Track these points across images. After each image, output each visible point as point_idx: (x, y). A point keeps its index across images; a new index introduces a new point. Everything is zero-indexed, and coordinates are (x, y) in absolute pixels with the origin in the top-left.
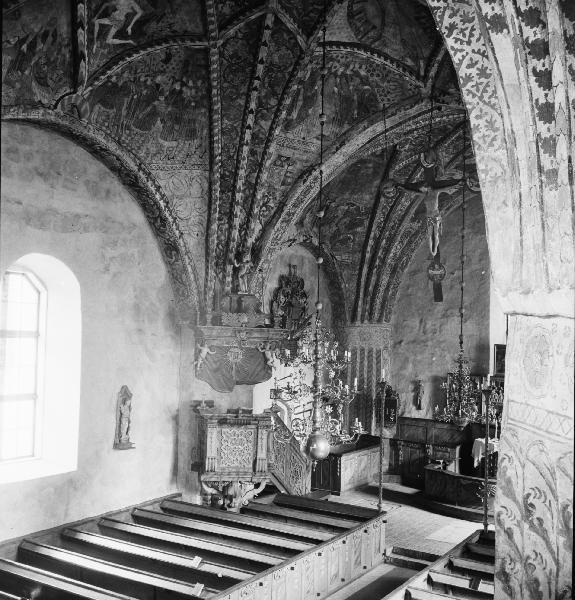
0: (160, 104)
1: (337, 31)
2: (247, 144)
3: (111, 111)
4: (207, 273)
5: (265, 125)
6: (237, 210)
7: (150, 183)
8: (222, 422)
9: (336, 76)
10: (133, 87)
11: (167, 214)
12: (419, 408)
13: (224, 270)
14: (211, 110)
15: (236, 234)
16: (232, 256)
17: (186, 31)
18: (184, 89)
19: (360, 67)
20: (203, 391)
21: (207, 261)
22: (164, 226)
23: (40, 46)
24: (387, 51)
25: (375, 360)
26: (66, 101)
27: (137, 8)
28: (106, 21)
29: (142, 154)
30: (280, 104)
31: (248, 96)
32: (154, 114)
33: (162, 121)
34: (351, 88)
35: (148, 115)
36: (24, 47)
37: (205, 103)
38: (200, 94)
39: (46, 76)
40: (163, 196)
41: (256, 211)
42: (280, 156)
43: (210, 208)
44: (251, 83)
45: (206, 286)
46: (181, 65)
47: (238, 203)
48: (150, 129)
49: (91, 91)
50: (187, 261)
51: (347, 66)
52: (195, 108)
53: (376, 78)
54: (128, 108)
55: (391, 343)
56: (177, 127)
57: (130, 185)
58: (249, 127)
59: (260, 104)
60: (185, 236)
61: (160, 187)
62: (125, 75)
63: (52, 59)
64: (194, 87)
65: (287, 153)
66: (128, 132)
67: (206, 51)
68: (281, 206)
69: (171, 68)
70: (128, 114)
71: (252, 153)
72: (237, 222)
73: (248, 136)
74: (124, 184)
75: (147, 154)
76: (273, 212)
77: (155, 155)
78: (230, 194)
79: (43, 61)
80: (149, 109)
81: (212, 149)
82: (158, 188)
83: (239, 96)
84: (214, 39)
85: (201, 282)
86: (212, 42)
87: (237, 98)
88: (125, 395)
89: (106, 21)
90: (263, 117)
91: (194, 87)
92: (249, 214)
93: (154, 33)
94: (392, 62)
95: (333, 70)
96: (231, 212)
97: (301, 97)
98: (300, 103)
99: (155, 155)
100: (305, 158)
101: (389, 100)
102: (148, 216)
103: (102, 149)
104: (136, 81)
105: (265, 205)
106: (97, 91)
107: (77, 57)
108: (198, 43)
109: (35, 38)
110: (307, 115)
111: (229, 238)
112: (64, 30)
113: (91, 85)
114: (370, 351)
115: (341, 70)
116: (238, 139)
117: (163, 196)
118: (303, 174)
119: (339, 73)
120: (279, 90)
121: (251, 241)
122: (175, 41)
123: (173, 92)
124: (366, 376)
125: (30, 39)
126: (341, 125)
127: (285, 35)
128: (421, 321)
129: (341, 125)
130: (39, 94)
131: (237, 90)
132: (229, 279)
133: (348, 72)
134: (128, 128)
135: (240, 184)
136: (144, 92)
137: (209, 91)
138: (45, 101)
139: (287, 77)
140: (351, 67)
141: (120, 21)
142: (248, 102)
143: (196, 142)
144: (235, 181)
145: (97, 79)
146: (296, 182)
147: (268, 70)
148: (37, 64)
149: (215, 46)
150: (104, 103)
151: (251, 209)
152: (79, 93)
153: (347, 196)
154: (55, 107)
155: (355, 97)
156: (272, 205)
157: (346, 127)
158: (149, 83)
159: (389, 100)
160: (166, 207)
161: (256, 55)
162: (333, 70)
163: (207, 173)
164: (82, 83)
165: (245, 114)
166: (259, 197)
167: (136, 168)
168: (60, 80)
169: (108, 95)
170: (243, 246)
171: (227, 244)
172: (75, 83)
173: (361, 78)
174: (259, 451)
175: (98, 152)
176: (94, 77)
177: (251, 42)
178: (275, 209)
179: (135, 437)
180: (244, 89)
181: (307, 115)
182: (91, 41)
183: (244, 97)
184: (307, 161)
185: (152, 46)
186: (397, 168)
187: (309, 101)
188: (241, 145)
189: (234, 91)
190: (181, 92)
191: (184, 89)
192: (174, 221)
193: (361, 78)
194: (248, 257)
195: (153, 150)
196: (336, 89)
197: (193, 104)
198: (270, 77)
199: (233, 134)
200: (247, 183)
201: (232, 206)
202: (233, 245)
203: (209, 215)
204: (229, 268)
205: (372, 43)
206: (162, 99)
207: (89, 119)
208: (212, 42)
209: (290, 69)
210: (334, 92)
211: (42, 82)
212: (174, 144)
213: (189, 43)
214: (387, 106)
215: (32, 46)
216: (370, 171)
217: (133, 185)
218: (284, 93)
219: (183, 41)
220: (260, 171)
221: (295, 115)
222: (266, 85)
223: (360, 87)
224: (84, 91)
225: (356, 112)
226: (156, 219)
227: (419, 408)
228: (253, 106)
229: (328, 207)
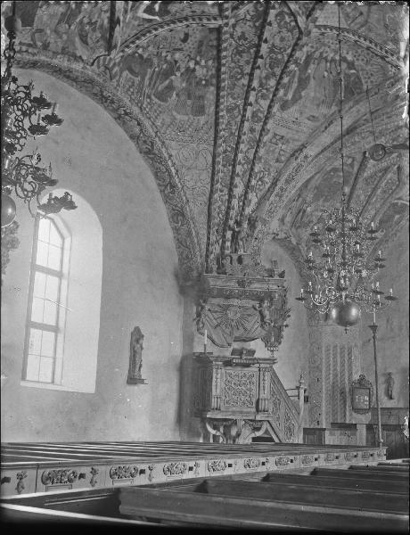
0: (177, 80)
1: (331, 16)
2: (248, 120)
3: (136, 79)
4: (209, 239)
5: (265, 104)
6: (237, 180)
7: (164, 150)
8: (228, 363)
9: (326, 59)
10: (155, 61)
11: (177, 180)
12: (391, 398)
13: (224, 236)
14: (218, 88)
15: (235, 202)
16: (231, 222)
17: (204, 12)
18: (197, 67)
20: (201, 345)
21: (209, 227)
22: (173, 192)
24: (372, 35)
25: (346, 355)
26: (101, 62)
29: (158, 123)
30: (278, 83)
31: (251, 75)
32: (170, 88)
33: (177, 95)
35: (167, 87)
37: (214, 81)
38: (210, 73)
40: (174, 164)
41: (253, 182)
42: (275, 135)
43: (212, 179)
44: (255, 63)
45: (207, 250)
46: (196, 45)
47: (238, 175)
48: (165, 101)
49: (122, 57)
50: (192, 226)
52: (205, 85)
54: (151, 79)
55: (360, 343)
56: (189, 102)
57: (146, 153)
58: (251, 104)
59: (261, 85)
60: (191, 204)
61: (171, 156)
62: (150, 48)
63: (93, 21)
64: (205, 67)
65: (282, 132)
66: (148, 100)
67: (219, 30)
68: (274, 184)
69: (187, 48)
70: (150, 83)
71: (252, 130)
72: (239, 191)
73: (249, 114)
74: (141, 152)
75: (163, 124)
76: (267, 186)
77: (169, 126)
78: (230, 168)
79: (86, 20)
80: (167, 82)
81: (217, 124)
82: (170, 156)
83: (243, 75)
84: (227, 17)
85: (204, 247)
86: (225, 21)
87: (241, 78)
88: (137, 336)
90: (264, 97)
91: (205, 67)
92: (247, 186)
93: (176, 11)
94: (376, 45)
95: (325, 55)
96: (231, 184)
97: (296, 80)
99: (169, 126)
100: (297, 137)
101: (372, 82)
102: (159, 185)
103: (126, 114)
104: (158, 55)
105: (260, 179)
106: (126, 58)
107: (114, 22)
108: (213, 21)
110: (301, 97)
111: (229, 208)
113: (123, 51)
114: (342, 348)
115: (332, 55)
116: (240, 117)
117: (174, 164)
118: (293, 155)
119: (329, 58)
120: (278, 71)
121: (248, 211)
122: (194, 20)
123: (188, 69)
124: (338, 369)
127: (287, 17)
128: (388, 321)
130: (81, 51)
131: (241, 70)
132: (228, 244)
133: (337, 58)
134: (149, 97)
135: (240, 156)
136: (164, 67)
137: (218, 70)
138: (85, 58)
139: (286, 58)
142: (251, 81)
143: (202, 119)
144: (236, 155)
145: (128, 47)
146: (288, 160)
147: (271, 50)
148: (81, 22)
149: (227, 24)
150: (132, 71)
151: (249, 181)
152: (112, 56)
153: (321, 203)
154: (93, 64)
156: (266, 180)
158: (169, 58)
159: (372, 82)
160: (176, 174)
161: (260, 38)
162: (325, 55)
163: (211, 149)
164: (115, 47)
165: (248, 92)
166: (256, 171)
167: (154, 135)
168: (98, 41)
169: (135, 63)
170: (242, 215)
171: (227, 213)
172: (110, 47)
174: (262, 391)
175: (121, 117)
176: (126, 44)
177: (257, 24)
178: (269, 185)
179: (144, 374)
180: (248, 69)
181: (301, 97)
182: (126, 12)
183: (247, 77)
184: (297, 140)
185: (174, 23)
186: (365, 174)
187: (303, 83)
188: (242, 122)
189: (240, 71)
190: (194, 70)
191: (197, 67)
192: (182, 188)
193: (348, 63)
194: (245, 225)
195: (168, 120)
196: (326, 74)
197: (204, 82)
198: (271, 58)
199: (236, 112)
200: (246, 157)
201: (232, 178)
202: (233, 213)
203: (212, 185)
204: (229, 234)
205: (359, 29)
206: (178, 74)
207: (118, 81)
208: (225, 21)
209: (289, 51)
211: (84, 40)
212: (186, 118)
213: (205, 21)
214: (370, 87)
216: (341, 181)
217: (149, 153)
218: (283, 73)
219: (201, 19)
220: (258, 146)
221: (290, 96)
222: (267, 66)
224: (116, 55)
226: (166, 186)
227: (391, 398)
228: (255, 84)
229: (305, 211)
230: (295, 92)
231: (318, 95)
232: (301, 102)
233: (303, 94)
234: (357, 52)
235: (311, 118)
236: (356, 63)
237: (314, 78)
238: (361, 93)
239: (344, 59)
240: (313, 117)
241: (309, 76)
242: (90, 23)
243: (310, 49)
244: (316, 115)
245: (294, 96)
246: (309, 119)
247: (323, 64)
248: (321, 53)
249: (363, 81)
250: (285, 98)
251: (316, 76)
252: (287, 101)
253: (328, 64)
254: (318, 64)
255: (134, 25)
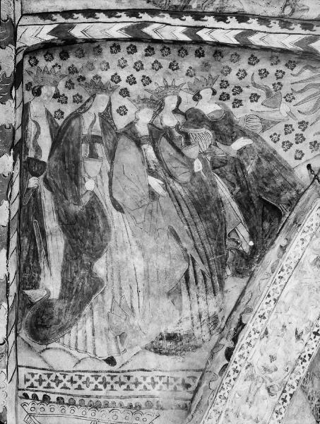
19: (197, 97)
34: (198, 166)
51: (158, 106)
53: (249, 107)
95: (121, 122)
97: (51, 223)
98: (57, 245)
110: (97, 285)
119: (142, 130)
126: (216, 287)
129: (216, 287)
133: (169, 120)
140: (171, 103)
155: (224, 191)
157: (233, 285)
162: (121, 122)
173: (213, 125)
181: (97, 285)
187: (85, 232)
193: (213, 125)
196: (155, 183)
210: (153, 195)
223: (221, 151)
225: (243, 232)
230: (65, 270)
231: (161, 262)
232: (104, 300)
233: (100, 268)
234: (224, 84)
235: (167, 345)
236: (238, 114)
237: (119, 208)
238: (300, 195)
239: (194, 118)
240: (171, 337)
241: (94, 207)
243: (53, 107)
244: (184, 328)
245: (67, 285)
246: (158, 351)
247: (129, 156)
248: (106, 118)
249: (287, 157)
250: (36, 295)
251: (126, 199)
252: (47, 303)
253: (149, 150)
254: (112, 155)
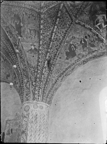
23: (86, 40)
27: (103, 15)
28: (99, 24)
36: (83, 42)
39: (94, 45)
79: (90, 42)
89: (99, 24)
109: (84, 39)
112: (90, 34)
125: (83, 40)
141: (102, 21)
148: (89, 43)
168: (98, 43)
211: (93, 46)
215: (84, 41)
242: (92, 41)
255: (104, 30)
